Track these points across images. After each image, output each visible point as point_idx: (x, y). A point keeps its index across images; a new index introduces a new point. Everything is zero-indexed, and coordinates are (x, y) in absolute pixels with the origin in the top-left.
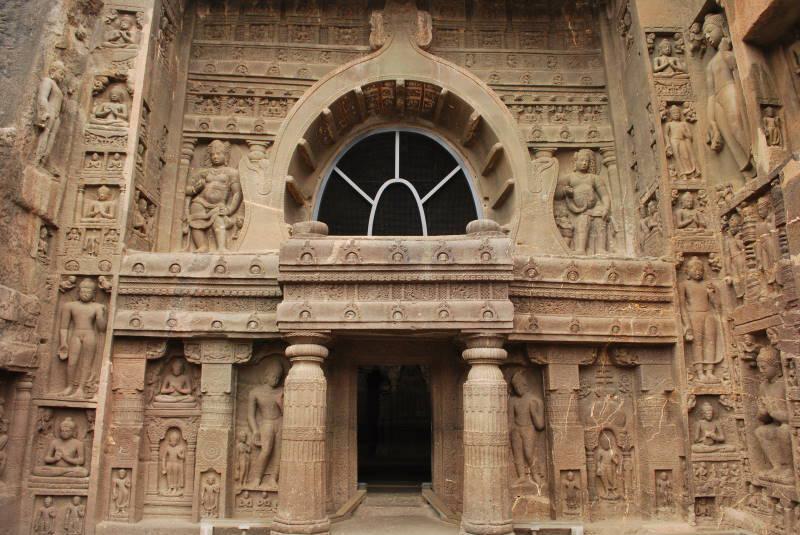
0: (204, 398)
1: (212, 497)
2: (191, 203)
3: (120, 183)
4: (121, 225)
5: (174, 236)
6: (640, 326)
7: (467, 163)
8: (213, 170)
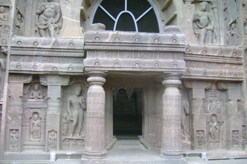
0: (49, 100)
1: (53, 142)
2: (39, 17)
3: (10, 5)
4: (11, 25)
5: (31, 32)
6: (230, 74)
7: (155, 5)
8: (48, 3)
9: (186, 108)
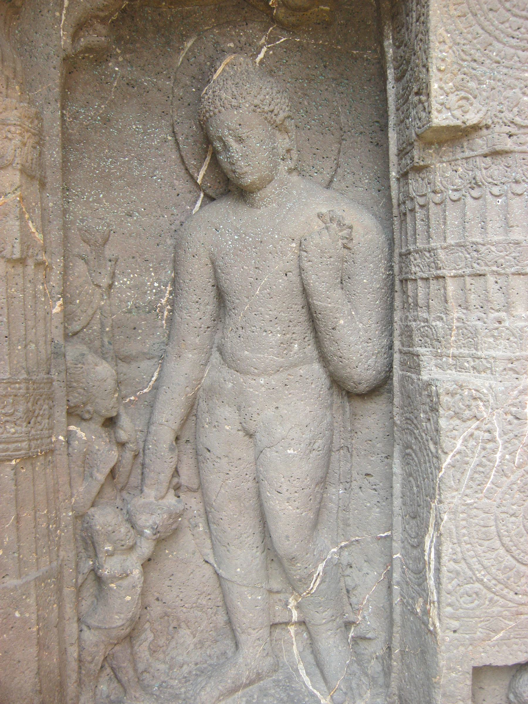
9: (328, 298)
